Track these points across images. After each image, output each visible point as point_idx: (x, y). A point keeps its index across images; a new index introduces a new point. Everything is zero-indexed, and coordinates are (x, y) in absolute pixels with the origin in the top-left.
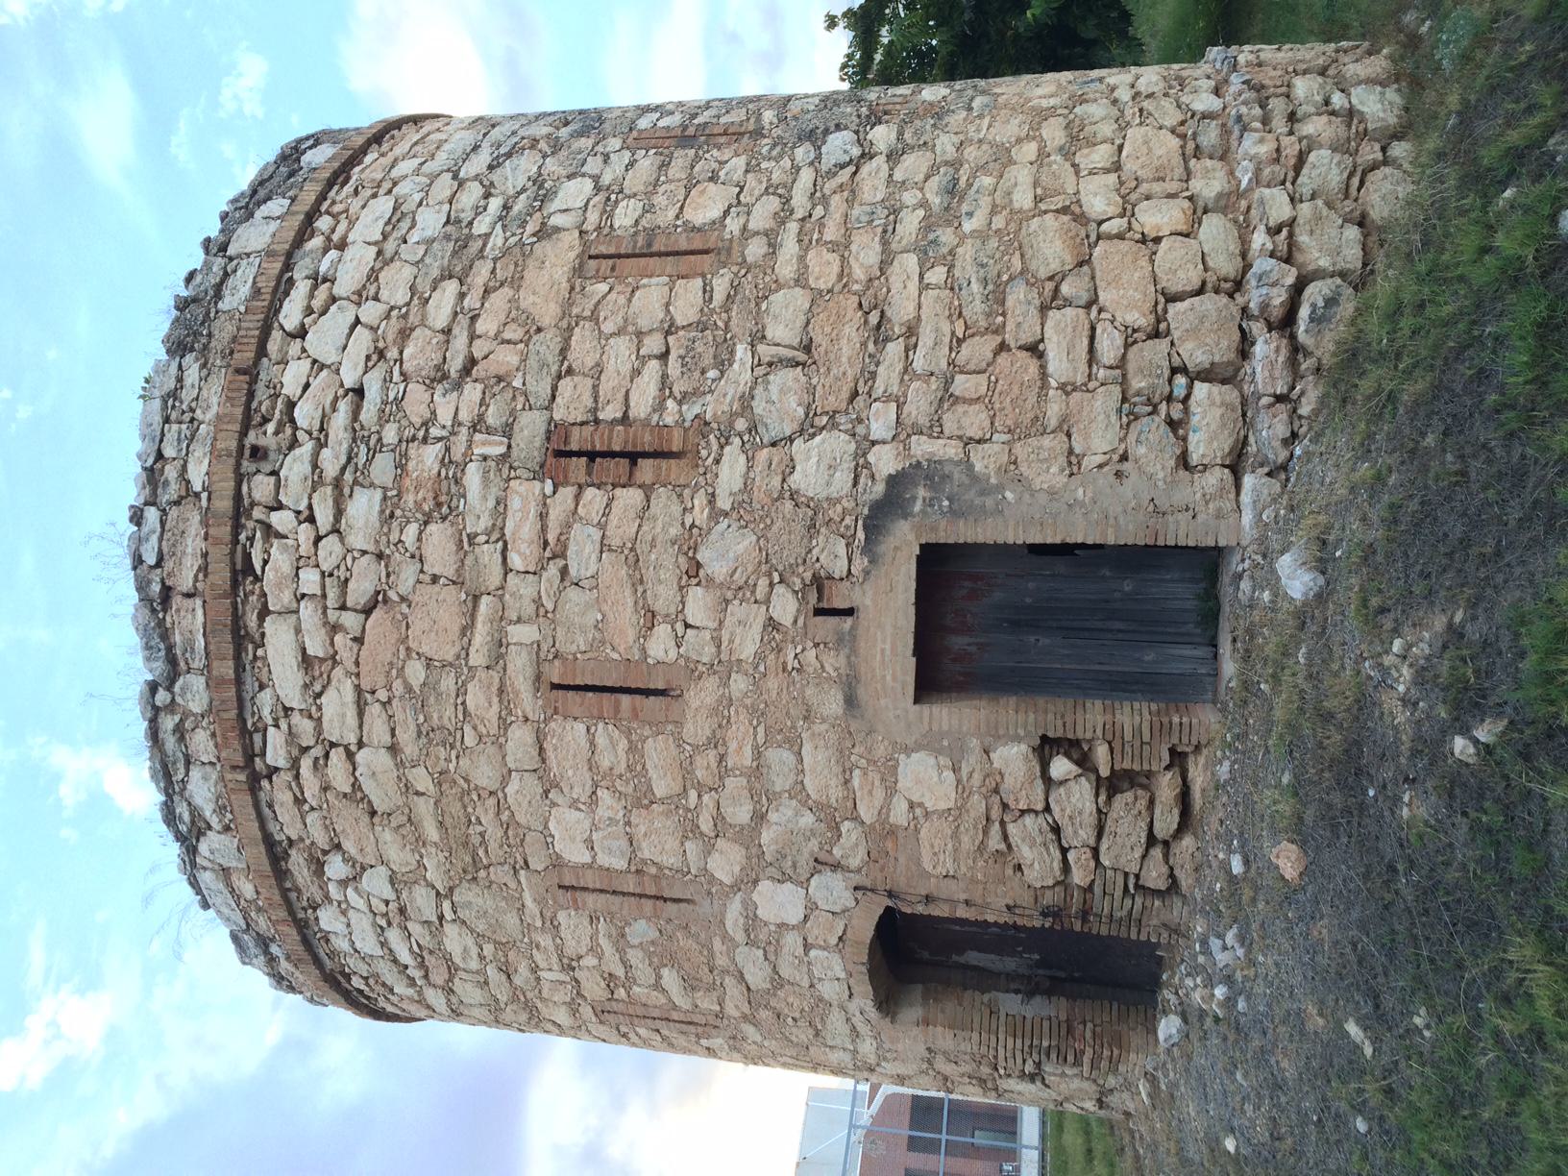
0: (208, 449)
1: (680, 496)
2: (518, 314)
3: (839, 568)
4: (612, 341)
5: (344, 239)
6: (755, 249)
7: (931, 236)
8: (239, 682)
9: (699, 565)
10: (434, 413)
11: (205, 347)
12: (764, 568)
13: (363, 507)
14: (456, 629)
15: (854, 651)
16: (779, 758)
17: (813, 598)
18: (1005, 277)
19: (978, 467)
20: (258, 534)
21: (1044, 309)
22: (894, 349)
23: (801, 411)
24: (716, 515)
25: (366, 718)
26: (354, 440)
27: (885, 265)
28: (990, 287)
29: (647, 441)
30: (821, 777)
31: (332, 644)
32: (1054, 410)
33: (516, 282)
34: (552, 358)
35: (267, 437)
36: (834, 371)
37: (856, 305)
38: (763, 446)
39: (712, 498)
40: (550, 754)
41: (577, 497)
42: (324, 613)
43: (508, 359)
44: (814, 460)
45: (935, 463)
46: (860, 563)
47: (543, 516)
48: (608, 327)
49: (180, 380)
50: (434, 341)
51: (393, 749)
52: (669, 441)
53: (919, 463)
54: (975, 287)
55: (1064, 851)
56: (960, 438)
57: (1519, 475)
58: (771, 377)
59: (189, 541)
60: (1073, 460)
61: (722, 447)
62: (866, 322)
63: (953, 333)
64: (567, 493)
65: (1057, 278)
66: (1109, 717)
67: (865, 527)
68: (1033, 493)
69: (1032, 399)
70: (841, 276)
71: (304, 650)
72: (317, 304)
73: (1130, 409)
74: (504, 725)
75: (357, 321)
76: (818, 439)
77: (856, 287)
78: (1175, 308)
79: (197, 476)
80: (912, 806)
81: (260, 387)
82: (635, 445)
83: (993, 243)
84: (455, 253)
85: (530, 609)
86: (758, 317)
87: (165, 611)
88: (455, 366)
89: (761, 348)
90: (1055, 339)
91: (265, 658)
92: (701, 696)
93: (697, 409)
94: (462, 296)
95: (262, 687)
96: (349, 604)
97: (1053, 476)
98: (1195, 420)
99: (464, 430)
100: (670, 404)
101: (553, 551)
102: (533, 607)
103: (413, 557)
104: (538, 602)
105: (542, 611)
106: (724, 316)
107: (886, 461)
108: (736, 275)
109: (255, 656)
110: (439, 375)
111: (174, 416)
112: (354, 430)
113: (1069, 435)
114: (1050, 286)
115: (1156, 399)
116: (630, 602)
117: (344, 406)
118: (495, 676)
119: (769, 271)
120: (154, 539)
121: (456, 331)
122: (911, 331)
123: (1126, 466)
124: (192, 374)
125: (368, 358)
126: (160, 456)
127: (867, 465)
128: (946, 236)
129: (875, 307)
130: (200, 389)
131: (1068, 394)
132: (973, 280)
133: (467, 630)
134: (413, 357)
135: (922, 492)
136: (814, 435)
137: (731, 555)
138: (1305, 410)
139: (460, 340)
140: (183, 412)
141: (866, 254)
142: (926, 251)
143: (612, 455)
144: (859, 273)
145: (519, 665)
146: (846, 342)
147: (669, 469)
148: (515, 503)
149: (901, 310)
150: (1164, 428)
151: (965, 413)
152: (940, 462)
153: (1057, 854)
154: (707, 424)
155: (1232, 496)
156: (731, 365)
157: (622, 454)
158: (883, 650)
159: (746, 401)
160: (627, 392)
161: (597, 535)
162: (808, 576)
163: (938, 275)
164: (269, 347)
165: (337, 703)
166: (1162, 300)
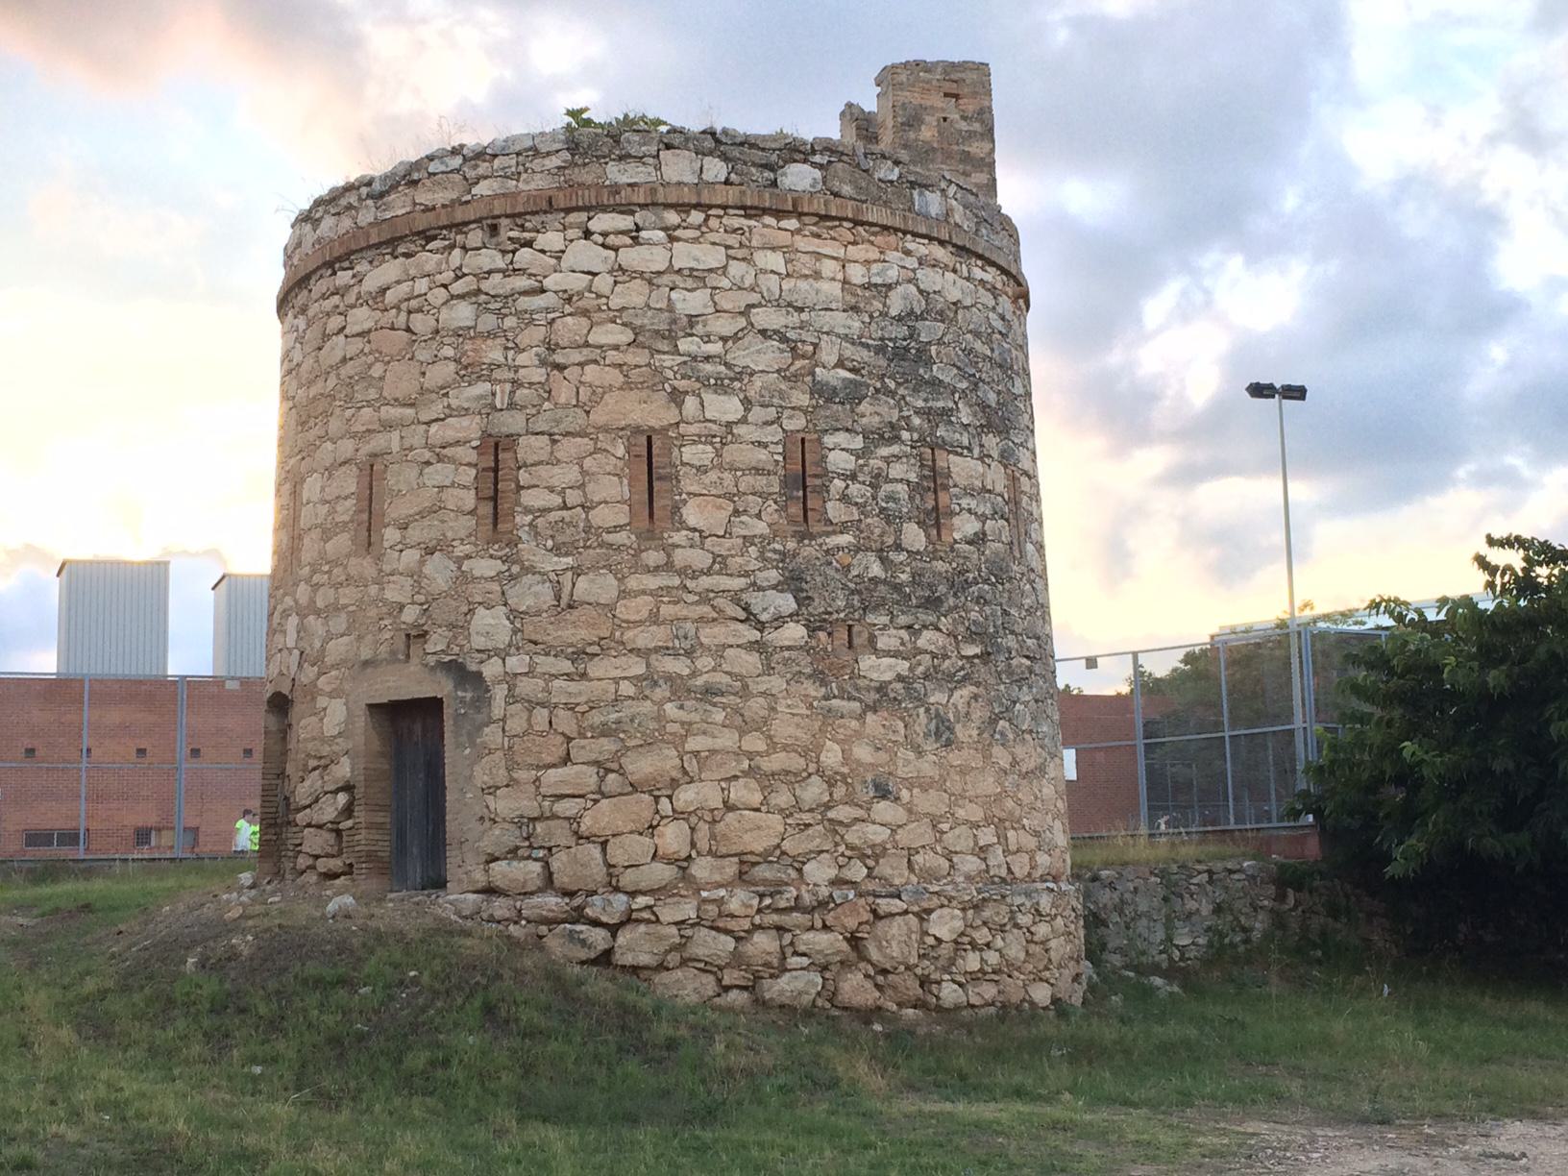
0: (498, 192)
1: (470, 535)
2: (598, 394)
3: (430, 648)
4: (576, 467)
5: (678, 239)
6: (653, 557)
7: (661, 682)
8: (369, 247)
9: (432, 554)
10: (524, 350)
11: (576, 165)
12: (430, 598)
13: (462, 314)
14: (398, 395)
15: (389, 662)
16: (339, 623)
17: (413, 633)
18: (622, 735)
19: (487, 730)
20: (447, 243)
21: (597, 763)
22: (566, 666)
23: (523, 608)
24: (459, 561)
25: (358, 339)
26: (506, 297)
27: (635, 651)
28: (614, 726)
29: (504, 506)
30: (338, 648)
31: (392, 308)
32: (522, 775)
33: (628, 386)
34: (563, 428)
35: (508, 232)
36: (551, 627)
37: (602, 635)
38: (502, 586)
39: (468, 557)
40: (343, 469)
41: (469, 464)
42: (406, 300)
43: (563, 395)
44: (492, 622)
45: (489, 702)
46: (431, 660)
47: (457, 443)
48: (588, 463)
49: (548, 154)
50: (577, 338)
51: (344, 360)
52: (504, 522)
53: (489, 691)
54: (614, 716)
55: (309, 806)
56: (505, 715)
57: (361, 1012)
58: (548, 584)
59: (441, 195)
60: (492, 790)
61: (500, 558)
62: (590, 644)
63: (578, 704)
64: (473, 456)
65: (621, 771)
66: (363, 825)
67: (451, 661)
68: (471, 766)
69: (529, 760)
70: (627, 622)
71: (389, 288)
72: (611, 240)
73: (526, 822)
74: (354, 436)
75: (594, 274)
76: (507, 622)
77: (618, 634)
78: (595, 851)
79: (483, 189)
80: (325, 709)
81: (543, 218)
82: (501, 498)
83: (652, 725)
84: (657, 332)
85: (407, 445)
86: (594, 568)
87: (406, 184)
88: (559, 358)
89: (569, 574)
90: (573, 772)
91: (384, 261)
92: (365, 566)
93: (524, 537)
94: (616, 348)
95: (371, 262)
96: (412, 316)
97: (481, 778)
98: (515, 863)
99: (512, 375)
100: (530, 517)
101: (440, 453)
102: (408, 446)
103: (436, 356)
104: (411, 449)
105: (407, 452)
106: (596, 544)
107: (491, 669)
108: (630, 547)
109: (384, 255)
110: (552, 347)
111: (521, 158)
112: (513, 295)
113: (507, 786)
114: (614, 766)
115: (532, 840)
116: (412, 512)
117: (532, 283)
118: (376, 426)
119: (633, 570)
120: (443, 168)
121: (585, 351)
122: (584, 676)
123: (487, 824)
124: (554, 162)
125: (565, 291)
126: (495, 156)
127: (490, 657)
128: (661, 692)
129: (602, 649)
130: (542, 172)
131: (534, 782)
132: (620, 714)
133: (398, 402)
134: (565, 325)
135: (469, 695)
136: (508, 618)
137: (436, 575)
138: (512, 927)
139: (576, 356)
140: (524, 165)
141: (643, 638)
142: (650, 679)
143: (496, 484)
144: (629, 634)
145: (377, 443)
146: (575, 632)
147: (486, 524)
148: (465, 422)
149: (596, 668)
150: (511, 845)
151: (521, 718)
152: (490, 705)
153: (308, 802)
154: (516, 545)
155: (471, 888)
156: (556, 555)
157: (496, 490)
158: (388, 681)
159: (530, 570)
160: (538, 486)
161: (447, 483)
162: (425, 628)
163: (627, 688)
164: (572, 215)
165: (362, 318)
166: (602, 839)
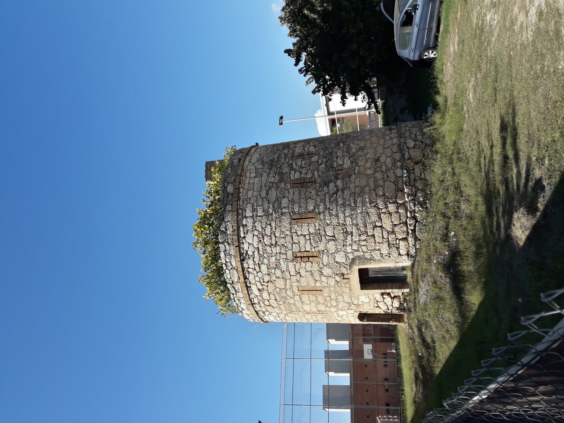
16: (340, 298)
30: (347, 299)
45: (359, 257)
46: (349, 272)
51: (276, 300)
55: (387, 306)
80: (362, 302)
88: (274, 243)
91: (252, 290)
92: (326, 291)
107: (351, 256)
117: (256, 251)
120: (229, 275)
124: (227, 246)
145: (295, 289)
146: (340, 237)
148: (290, 265)
157: (306, 257)
